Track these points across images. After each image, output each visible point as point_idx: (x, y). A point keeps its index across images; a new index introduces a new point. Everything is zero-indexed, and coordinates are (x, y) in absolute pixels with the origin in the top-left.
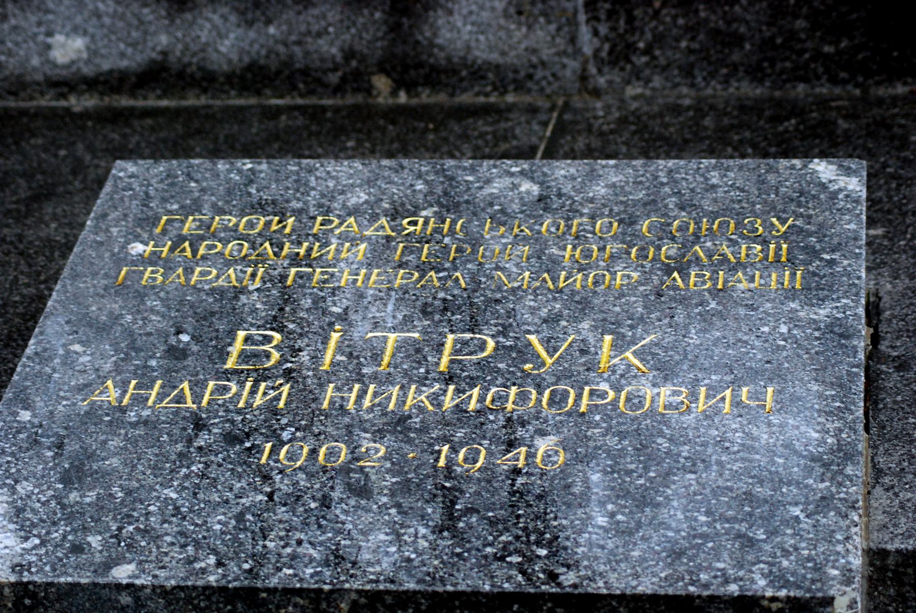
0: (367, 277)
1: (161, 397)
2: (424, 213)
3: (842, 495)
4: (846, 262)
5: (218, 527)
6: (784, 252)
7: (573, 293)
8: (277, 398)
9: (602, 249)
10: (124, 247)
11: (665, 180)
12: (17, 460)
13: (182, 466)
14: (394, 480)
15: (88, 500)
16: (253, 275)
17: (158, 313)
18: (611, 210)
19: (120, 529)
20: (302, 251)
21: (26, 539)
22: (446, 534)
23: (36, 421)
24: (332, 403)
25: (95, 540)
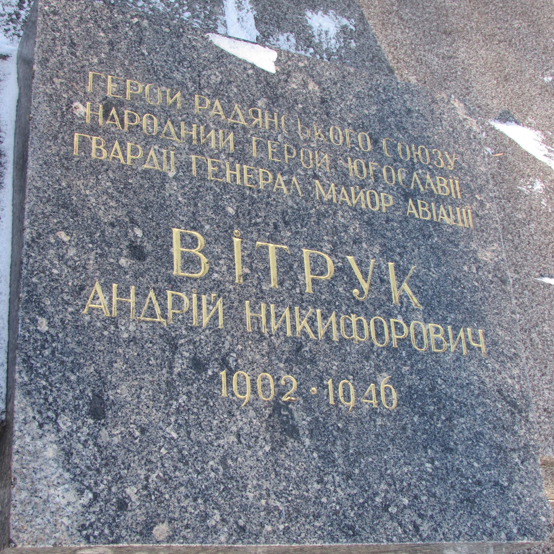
0: (242, 171)
1: (139, 305)
5: (212, 475)
7: (363, 213)
8: (215, 317)
9: (367, 166)
10: (69, 106)
12: (50, 385)
13: (172, 398)
14: (309, 419)
15: (116, 440)
16: (168, 158)
19: (147, 478)
20: (194, 133)
21: (81, 492)
22: (350, 481)
23: (53, 331)
24: (253, 324)
25: (131, 491)
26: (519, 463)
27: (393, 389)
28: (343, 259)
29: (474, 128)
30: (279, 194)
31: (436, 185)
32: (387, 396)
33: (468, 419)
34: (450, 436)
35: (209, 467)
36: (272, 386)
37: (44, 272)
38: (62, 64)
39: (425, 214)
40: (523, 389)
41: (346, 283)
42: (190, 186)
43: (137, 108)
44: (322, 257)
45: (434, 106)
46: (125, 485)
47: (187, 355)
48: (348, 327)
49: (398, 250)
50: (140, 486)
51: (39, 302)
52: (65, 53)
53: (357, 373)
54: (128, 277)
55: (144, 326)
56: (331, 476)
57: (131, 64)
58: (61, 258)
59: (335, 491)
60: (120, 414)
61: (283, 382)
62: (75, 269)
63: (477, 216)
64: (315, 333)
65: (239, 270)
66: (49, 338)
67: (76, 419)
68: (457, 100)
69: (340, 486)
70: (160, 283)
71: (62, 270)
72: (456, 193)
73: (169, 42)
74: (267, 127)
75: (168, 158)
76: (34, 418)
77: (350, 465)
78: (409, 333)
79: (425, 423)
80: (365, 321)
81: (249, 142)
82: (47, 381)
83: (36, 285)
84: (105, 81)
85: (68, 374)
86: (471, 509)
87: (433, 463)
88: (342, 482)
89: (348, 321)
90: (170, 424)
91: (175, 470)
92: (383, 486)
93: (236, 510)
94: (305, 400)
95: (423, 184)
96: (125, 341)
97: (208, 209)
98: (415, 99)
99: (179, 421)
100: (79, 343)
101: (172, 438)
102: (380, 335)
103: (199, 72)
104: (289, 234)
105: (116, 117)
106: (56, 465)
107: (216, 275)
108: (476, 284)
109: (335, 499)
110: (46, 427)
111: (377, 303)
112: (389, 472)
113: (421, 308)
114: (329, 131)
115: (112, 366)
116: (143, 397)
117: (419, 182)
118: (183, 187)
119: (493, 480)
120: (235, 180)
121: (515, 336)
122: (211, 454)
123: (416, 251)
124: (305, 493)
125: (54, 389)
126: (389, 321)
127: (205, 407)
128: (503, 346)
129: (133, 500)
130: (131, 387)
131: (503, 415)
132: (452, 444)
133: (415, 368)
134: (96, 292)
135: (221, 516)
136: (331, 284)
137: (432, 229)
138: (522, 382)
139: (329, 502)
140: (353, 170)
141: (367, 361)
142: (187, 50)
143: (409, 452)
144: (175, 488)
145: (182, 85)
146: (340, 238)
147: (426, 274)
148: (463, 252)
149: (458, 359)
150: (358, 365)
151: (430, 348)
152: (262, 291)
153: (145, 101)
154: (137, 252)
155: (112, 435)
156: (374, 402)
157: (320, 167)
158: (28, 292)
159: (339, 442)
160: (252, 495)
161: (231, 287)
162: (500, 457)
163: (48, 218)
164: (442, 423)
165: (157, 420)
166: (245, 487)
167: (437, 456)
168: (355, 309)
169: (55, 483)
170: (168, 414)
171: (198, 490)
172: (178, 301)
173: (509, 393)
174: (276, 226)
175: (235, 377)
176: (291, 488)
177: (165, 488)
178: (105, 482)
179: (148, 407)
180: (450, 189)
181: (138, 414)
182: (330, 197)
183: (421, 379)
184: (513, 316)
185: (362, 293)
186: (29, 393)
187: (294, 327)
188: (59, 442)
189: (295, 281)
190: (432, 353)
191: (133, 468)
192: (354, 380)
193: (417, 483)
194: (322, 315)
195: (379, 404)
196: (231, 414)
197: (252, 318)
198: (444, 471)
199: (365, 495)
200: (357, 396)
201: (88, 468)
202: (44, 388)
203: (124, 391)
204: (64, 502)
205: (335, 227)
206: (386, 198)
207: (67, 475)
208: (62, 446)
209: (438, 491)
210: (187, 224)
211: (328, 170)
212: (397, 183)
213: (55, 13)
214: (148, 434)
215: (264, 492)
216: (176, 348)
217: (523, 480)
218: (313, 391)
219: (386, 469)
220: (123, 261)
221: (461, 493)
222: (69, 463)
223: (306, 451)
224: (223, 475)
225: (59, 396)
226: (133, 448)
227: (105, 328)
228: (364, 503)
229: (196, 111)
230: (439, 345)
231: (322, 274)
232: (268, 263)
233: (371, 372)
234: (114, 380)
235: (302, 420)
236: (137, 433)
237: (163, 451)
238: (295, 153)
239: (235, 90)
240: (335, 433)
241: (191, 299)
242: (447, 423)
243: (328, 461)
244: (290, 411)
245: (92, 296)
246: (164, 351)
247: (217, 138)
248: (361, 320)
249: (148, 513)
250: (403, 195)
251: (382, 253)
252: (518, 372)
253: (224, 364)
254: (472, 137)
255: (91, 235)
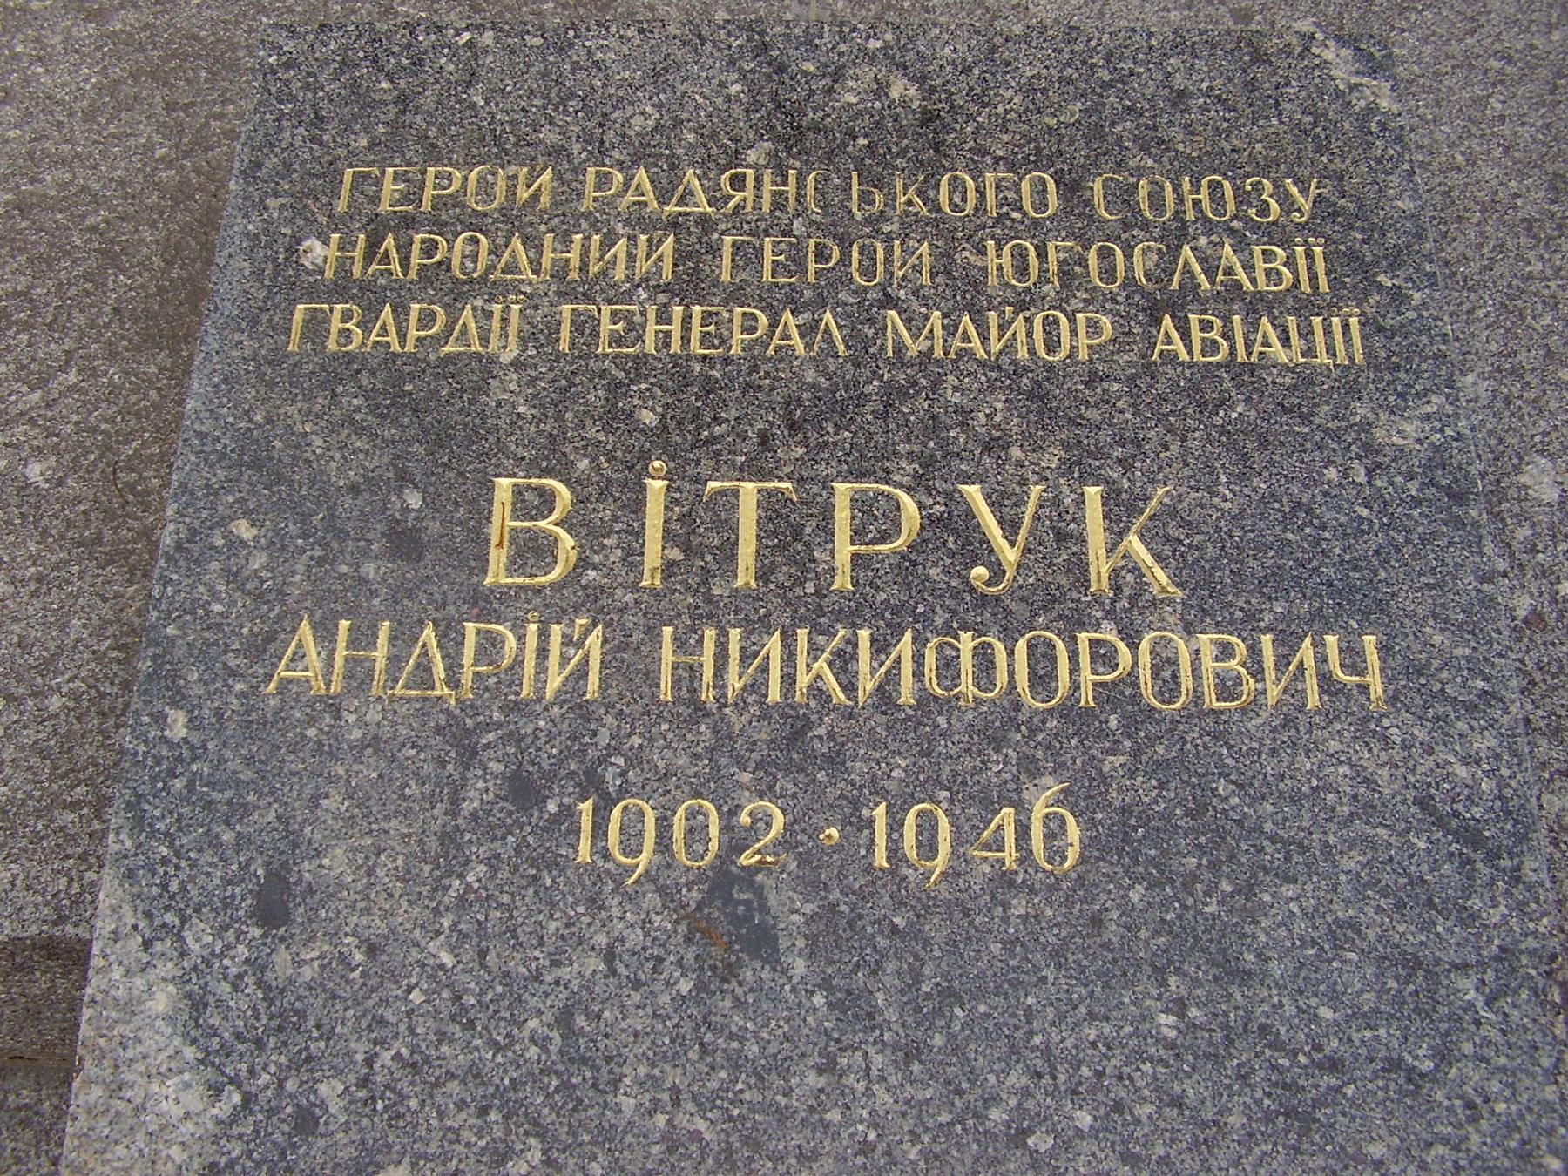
0: (687, 320)
1: (395, 662)
2: (752, 156)
3: (1531, 943)
4: (1417, 296)
5: (533, 1052)
6: (1320, 266)
7: (1019, 370)
8: (581, 673)
9: (1042, 254)
10: (291, 251)
11: (1107, 77)
12: (178, 855)
14: (809, 908)
15: (307, 973)
16: (505, 320)
17: (360, 430)
18: (1038, 150)
19: (369, 1062)
20: (574, 257)
21: (216, 1091)
22: (916, 1067)
23: (195, 738)
24: (676, 683)
25: (329, 1090)
26: (1480, 1004)
27: (1070, 820)
28: (949, 496)
29: (1384, 104)
30: (781, 360)
31: (1249, 268)
32: (1049, 837)
33: (1309, 887)
34: (1245, 936)
35: (526, 1033)
36: (714, 831)
37: (193, 612)
38: (288, 166)
39: (1210, 347)
40: (1508, 792)
41: (952, 555)
42: (551, 376)
43: (446, 224)
44: (888, 496)
45: (1260, 72)
46: (318, 1075)
47: (495, 767)
48: (947, 665)
49: (1119, 452)
50: (352, 1078)
51: (175, 676)
52: (298, 141)
53: (964, 783)
54: (376, 601)
55: (404, 710)
56: (858, 1055)
57: (442, 131)
58: (231, 575)
59: (869, 1093)
60: (323, 914)
61: (744, 819)
62: (260, 597)
63: (1380, 329)
64: (850, 688)
65: (654, 552)
66: (186, 753)
67: (225, 928)
68: (1331, 43)
69: (884, 1079)
70: (452, 609)
71: (233, 603)
72: (1313, 278)
73: (539, 66)
74: (766, 208)
75: (505, 320)
76: (135, 927)
77: (919, 1024)
78: (1135, 664)
79: (1165, 905)
80: (999, 646)
81: (715, 251)
82: (171, 846)
83: (172, 640)
84: (378, 183)
85: (218, 829)
86: (1299, 1139)
87: (1181, 1015)
88: (891, 1070)
89: (948, 652)
90: (438, 933)
91: (440, 1042)
92: (1017, 1079)
93: (586, 1138)
94: (803, 860)
95: (1210, 272)
96: (352, 748)
97: (589, 422)
98: (1200, 64)
99: (462, 926)
100: (249, 760)
101: (442, 967)
102: (1042, 679)
103: (605, 115)
104: (800, 451)
105: (394, 254)
106: (170, 1030)
107: (592, 574)
108: (1365, 513)
109: (865, 1114)
110: (158, 947)
111: (1040, 596)
112: (1037, 1040)
113: (1180, 594)
114: (937, 185)
115: (318, 806)
116: (380, 873)
117: (1197, 268)
118: (533, 380)
119: (1383, 1053)
120: (667, 345)
121: (1490, 642)
122: (533, 1002)
123: (1175, 447)
124: (779, 1098)
125: (183, 864)
126: (1074, 638)
127: (531, 891)
128: (1445, 675)
129: (332, 1110)
130: (355, 850)
131: (1432, 871)
132: (1251, 957)
133: (1144, 758)
134: (300, 645)
135: (545, 1152)
136: (908, 563)
137: (1227, 384)
138: (1505, 772)
139: (849, 1121)
140: (1000, 268)
141: (997, 750)
142: (581, 74)
143: (1106, 985)
144: (436, 1085)
145: (557, 153)
146: (943, 444)
147: (1203, 506)
148: (1326, 431)
149: (1288, 722)
150: (969, 763)
151: (1198, 697)
152: (709, 599)
153: (464, 206)
154: (405, 542)
155: (297, 963)
156: (1010, 855)
157: (904, 278)
158: (155, 658)
159: (890, 966)
160: (632, 1101)
161: (629, 598)
162: (1411, 988)
163: (216, 494)
164: (1222, 902)
165: (408, 926)
166: (616, 1083)
167: (1199, 992)
168: (970, 617)
169: (163, 1069)
170: (436, 911)
171: (491, 1090)
172: (489, 643)
173: (1459, 807)
174: (765, 439)
175: (617, 811)
176: (740, 1086)
177: (412, 1083)
178: (273, 1069)
179: (391, 896)
180: (1295, 272)
181: (367, 911)
182: (923, 345)
183: (1161, 786)
184: (1485, 586)
185: (997, 573)
186: (130, 874)
187: (789, 680)
188: (182, 980)
189: (804, 566)
190: (1204, 714)
191: (340, 1036)
192: (951, 801)
193: (1126, 1070)
194: (873, 641)
195: (1021, 861)
196: (596, 904)
197: (675, 667)
198: (1218, 1036)
199: (958, 1103)
200: (957, 841)
201: (239, 1037)
202: (165, 861)
203: (337, 861)
204: (177, 1112)
205: (933, 418)
206: (1093, 326)
207: (190, 1053)
208: (188, 988)
209: (1191, 1090)
210: (534, 463)
211: (926, 279)
212: (1129, 281)
213: (288, 66)
214: (384, 958)
215: (665, 1097)
216: (475, 753)
217: (1489, 1052)
218: (829, 837)
219: (1031, 1033)
220: (369, 569)
221: (1269, 1095)
222: (197, 1026)
223: (793, 990)
224: (561, 1052)
225: (192, 879)
226: (346, 992)
227: (312, 721)
228: (952, 1124)
229: (587, 204)
230: (1227, 688)
231: (883, 538)
232: (735, 531)
233: (1008, 776)
234: (318, 836)
235: (791, 911)
236: (359, 957)
237: (416, 997)
238: (836, 254)
239: (691, 137)
240: (882, 942)
241: (521, 639)
242: (1240, 900)
243: (856, 1016)
244: (759, 891)
245: (289, 653)
246: (443, 764)
247: (631, 257)
248: (990, 645)
249: (363, 1141)
250: (1144, 310)
251: (1067, 467)
252: (1494, 742)
253: (591, 783)
254: (1374, 127)
255: (305, 518)
